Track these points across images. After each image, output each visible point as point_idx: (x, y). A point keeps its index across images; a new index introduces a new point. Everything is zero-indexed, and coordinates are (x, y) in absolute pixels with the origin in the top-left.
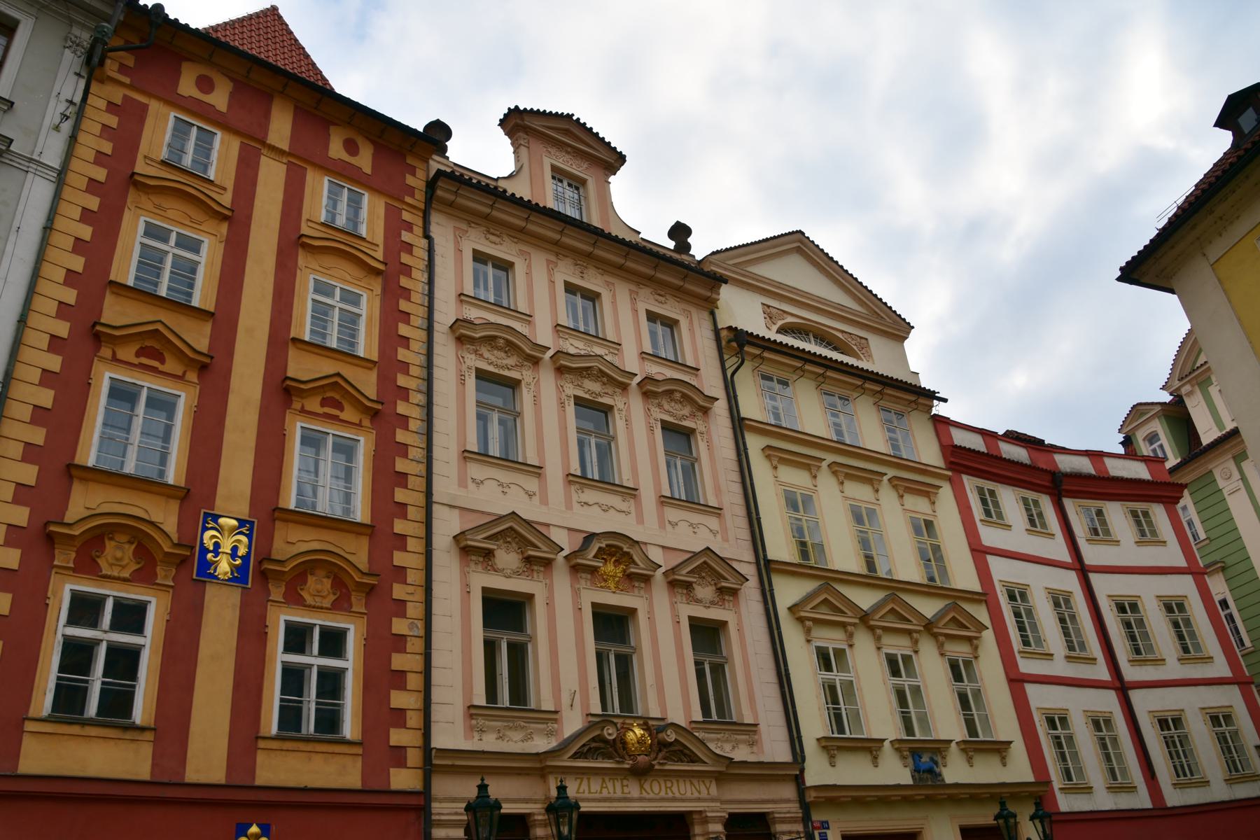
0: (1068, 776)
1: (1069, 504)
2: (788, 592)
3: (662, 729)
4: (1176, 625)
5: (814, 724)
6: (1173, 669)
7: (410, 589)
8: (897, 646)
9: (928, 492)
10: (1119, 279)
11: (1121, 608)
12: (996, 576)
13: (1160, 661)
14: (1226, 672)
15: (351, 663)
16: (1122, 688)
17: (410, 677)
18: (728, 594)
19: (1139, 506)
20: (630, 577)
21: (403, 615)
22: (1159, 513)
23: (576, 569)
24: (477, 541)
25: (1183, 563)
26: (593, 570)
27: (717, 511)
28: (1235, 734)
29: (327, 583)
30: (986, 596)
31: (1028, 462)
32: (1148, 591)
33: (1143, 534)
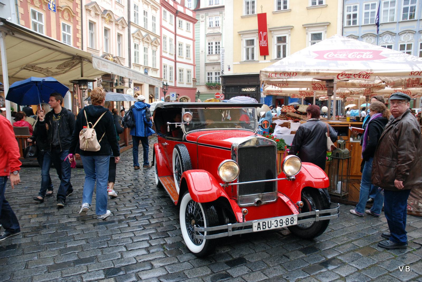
0: (164, 78)
1: (177, 18)
2: (133, 30)
3: (115, 58)
4: (187, 51)
5: (133, 61)
6: (184, 60)
7: (79, 18)
8: (146, 45)
9: (156, 9)
11: (179, 45)
12: (163, 33)
13: (183, 58)
15: (71, 34)
16: (176, 62)
17: (79, 39)
18: (123, 28)
19: (189, 22)
20: (110, 21)
21: (78, 24)
22: (191, 24)
23: (102, 17)
24: (90, 8)
25: (192, 38)
26: (105, 18)
27: (123, 7)
28: (190, 75)
29: (67, 14)
30: (160, 37)
31: (173, 6)
32: (185, 42)
33: (187, 29)
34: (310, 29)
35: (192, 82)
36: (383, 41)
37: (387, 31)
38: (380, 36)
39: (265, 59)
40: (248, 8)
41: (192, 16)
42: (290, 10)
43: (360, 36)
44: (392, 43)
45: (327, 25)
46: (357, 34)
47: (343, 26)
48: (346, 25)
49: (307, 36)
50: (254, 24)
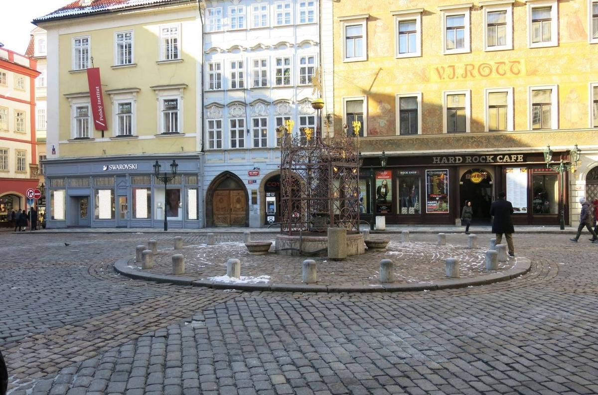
10: (32, 23)
14: (29, 139)
22: (27, 79)
34: (161, 93)
35: (28, 169)
36: (255, 112)
37: (259, 99)
38: (251, 106)
39: (103, 136)
40: (122, 54)
41: (28, 65)
42: (135, 65)
43: (226, 104)
44: (265, 116)
45: (182, 87)
46: (222, 103)
47: (203, 89)
48: (207, 88)
49: (158, 103)
50: (82, 84)
